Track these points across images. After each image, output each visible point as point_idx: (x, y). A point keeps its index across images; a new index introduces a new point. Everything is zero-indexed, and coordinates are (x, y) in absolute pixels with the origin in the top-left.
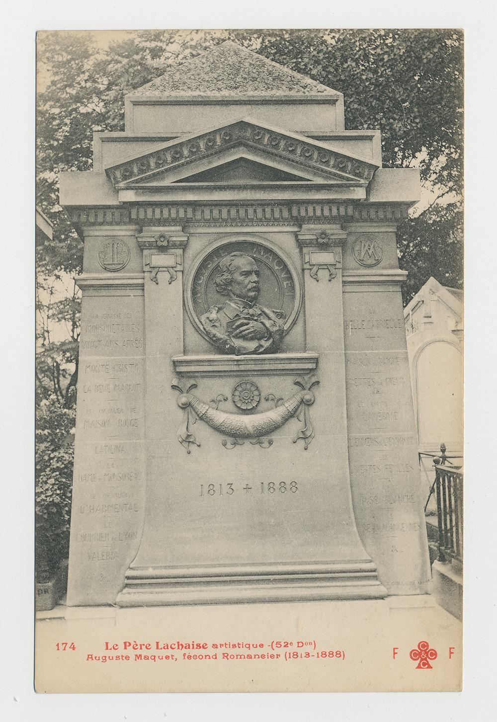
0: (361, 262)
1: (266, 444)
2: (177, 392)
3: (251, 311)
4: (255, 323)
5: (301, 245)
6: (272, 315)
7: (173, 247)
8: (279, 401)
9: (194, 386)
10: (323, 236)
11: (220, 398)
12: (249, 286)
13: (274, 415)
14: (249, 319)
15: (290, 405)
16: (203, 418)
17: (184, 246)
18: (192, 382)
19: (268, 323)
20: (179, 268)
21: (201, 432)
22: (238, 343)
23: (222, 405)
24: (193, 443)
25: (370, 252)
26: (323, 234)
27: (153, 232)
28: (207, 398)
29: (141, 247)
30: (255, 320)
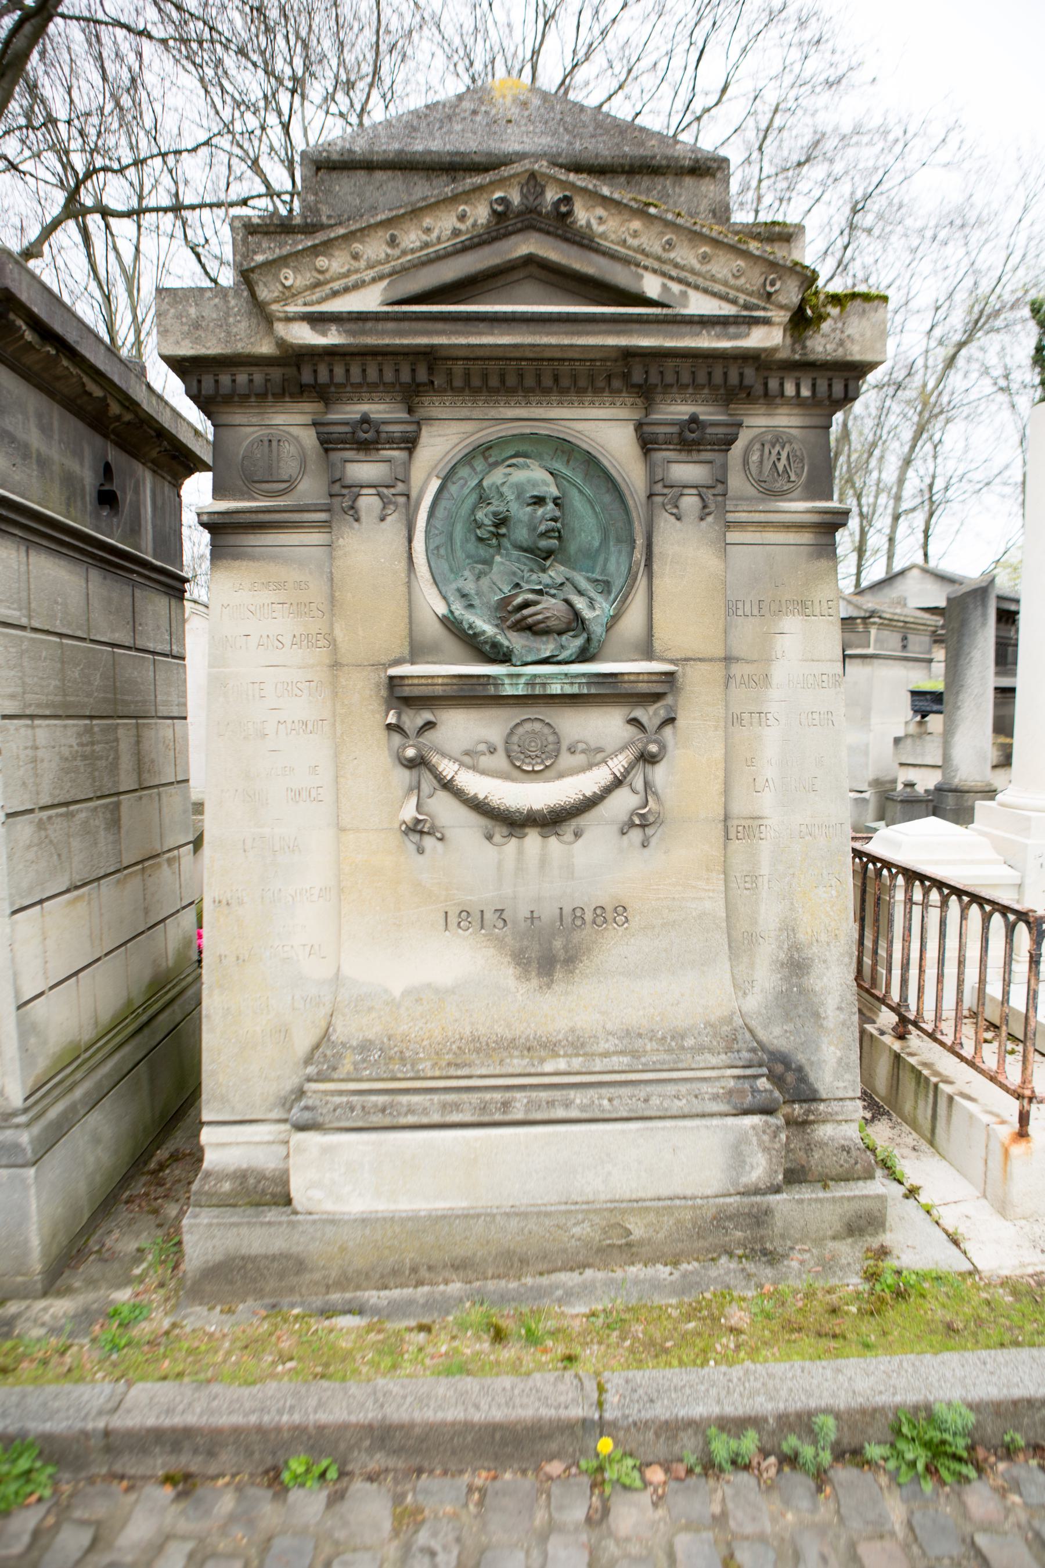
1: (569, 836)
2: (397, 738)
3: (545, 578)
4: (554, 601)
5: (647, 444)
6: (584, 584)
8: (595, 756)
9: (429, 725)
10: (694, 426)
11: (482, 747)
12: (542, 528)
13: (590, 782)
14: (540, 592)
15: (618, 764)
16: (447, 786)
17: (410, 443)
18: (427, 716)
19: (580, 603)
20: (400, 487)
21: (445, 810)
22: (515, 641)
24: (428, 833)
25: (781, 468)
26: (694, 419)
29: (328, 443)
30: (553, 596)
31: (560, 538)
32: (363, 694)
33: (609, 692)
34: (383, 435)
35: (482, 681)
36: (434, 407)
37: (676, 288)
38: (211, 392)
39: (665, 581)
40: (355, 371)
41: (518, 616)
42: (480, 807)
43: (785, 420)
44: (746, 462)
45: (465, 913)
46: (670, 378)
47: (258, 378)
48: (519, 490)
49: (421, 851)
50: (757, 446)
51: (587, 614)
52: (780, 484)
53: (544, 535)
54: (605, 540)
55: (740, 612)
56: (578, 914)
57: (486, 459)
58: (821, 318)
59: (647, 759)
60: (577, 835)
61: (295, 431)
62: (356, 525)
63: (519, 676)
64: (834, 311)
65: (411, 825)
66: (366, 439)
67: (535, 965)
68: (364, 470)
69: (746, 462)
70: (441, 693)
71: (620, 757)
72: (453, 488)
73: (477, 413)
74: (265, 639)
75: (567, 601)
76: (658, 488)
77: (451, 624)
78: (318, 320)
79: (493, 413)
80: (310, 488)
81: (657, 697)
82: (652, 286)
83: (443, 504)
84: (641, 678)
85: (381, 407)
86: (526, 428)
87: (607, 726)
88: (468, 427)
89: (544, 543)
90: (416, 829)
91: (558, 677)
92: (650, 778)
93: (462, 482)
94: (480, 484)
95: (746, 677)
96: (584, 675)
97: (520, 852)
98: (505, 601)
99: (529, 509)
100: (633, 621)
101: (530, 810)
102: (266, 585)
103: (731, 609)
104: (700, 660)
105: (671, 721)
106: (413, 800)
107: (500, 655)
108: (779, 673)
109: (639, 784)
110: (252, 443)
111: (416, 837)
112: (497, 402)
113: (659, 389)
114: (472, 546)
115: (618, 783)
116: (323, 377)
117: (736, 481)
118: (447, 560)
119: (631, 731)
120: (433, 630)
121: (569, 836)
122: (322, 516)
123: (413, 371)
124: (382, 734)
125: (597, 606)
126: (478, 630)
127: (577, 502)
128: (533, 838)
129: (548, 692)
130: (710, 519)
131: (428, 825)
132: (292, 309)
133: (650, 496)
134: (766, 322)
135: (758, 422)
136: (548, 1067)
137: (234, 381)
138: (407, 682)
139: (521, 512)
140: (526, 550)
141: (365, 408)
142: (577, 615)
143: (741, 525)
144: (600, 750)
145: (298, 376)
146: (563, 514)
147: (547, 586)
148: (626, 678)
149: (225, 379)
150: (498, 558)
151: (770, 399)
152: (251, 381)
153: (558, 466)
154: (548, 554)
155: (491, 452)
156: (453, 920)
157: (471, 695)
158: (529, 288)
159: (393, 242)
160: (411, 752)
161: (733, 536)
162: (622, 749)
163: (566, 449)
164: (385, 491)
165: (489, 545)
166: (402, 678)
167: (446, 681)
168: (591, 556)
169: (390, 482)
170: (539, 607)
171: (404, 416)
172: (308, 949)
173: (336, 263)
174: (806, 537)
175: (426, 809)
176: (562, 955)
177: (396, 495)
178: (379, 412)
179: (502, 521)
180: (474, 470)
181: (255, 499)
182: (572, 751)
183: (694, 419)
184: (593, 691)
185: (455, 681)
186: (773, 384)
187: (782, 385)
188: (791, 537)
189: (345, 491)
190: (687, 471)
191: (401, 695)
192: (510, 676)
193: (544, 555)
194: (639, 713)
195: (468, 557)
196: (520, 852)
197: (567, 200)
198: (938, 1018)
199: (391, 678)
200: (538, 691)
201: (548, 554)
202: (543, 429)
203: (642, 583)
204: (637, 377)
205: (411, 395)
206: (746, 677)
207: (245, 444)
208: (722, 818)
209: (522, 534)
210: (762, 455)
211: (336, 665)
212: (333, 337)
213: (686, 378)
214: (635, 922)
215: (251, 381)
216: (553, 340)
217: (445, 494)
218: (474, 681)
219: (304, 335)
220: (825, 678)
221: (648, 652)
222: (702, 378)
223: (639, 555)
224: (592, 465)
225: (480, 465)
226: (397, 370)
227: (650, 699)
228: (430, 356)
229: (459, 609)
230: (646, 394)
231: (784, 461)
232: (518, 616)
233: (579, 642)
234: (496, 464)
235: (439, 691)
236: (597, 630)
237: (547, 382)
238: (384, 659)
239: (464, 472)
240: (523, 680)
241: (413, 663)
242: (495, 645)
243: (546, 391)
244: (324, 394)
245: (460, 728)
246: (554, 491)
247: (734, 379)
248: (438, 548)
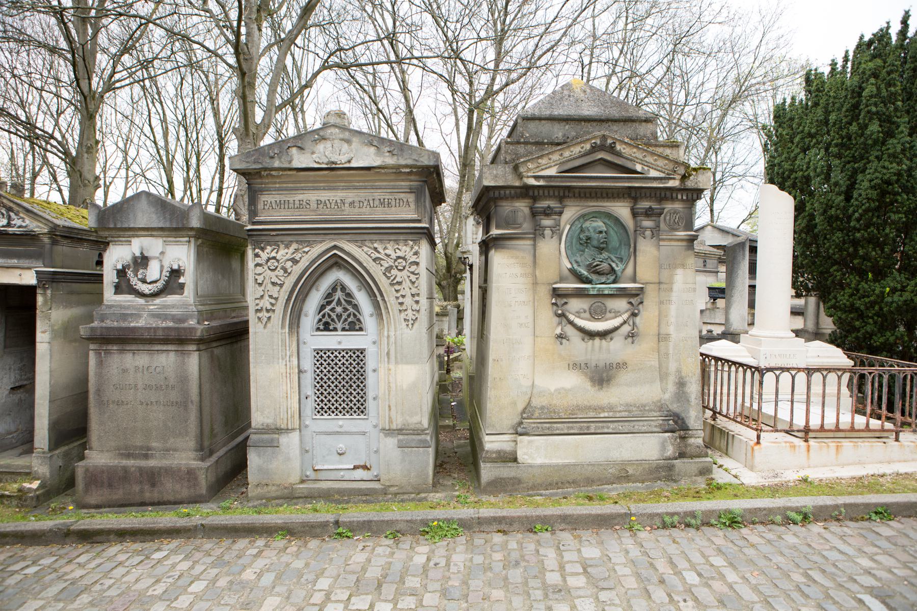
2: (555, 307)
5: (634, 214)
6: (614, 259)
8: (617, 314)
9: (566, 303)
13: (616, 322)
15: (625, 316)
16: (571, 323)
17: (560, 213)
18: (565, 300)
19: (614, 265)
21: (570, 330)
22: (594, 277)
23: (583, 315)
26: (650, 208)
27: (543, 204)
28: (573, 310)
29: (534, 213)
32: (544, 292)
33: (623, 293)
36: (568, 202)
37: (646, 168)
39: (640, 258)
40: (546, 192)
43: (678, 206)
44: (665, 219)
46: (643, 195)
47: (513, 192)
48: (595, 229)
49: (561, 344)
51: (616, 269)
52: (676, 226)
54: (620, 244)
56: (611, 365)
58: (690, 175)
59: (634, 315)
60: (611, 339)
64: (694, 173)
66: (548, 212)
68: (546, 222)
69: (665, 219)
72: (573, 228)
73: (581, 204)
77: (573, 271)
78: (537, 178)
79: (586, 204)
81: (637, 295)
82: (639, 168)
87: (621, 304)
88: (578, 208)
89: (602, 246)
90: (560, 337)
91: (607, 288)
97: (593, 344)
98: (591, 264)
100: (629, 270)
103: (661, 267)
105: (642, 303)
107: (589, 281)
108: (676, 287)
109: (631, 323)
114: (578, 246)
115: (625, 322)
116: (536, 193)
117: (662, 225)
119: (628, 306)
120: (566, 272)
121: (609, 340)
124: (550, 306)
127: (612, 232)
128: (597, 340)
132: (529, 174)
133: (635, 231)
134: (674, 179)
135: (669, 206)
136: (602, 415)
142: (613, 269)
143: (663, 240)
145: (526, 192)
149: (502, 192)
151: (673, 199)
153: (606, 221)
154: (603, 249)
156: (571, 366)
157: (580, 294)
158: (600, 167)
159: (561, 155)
160: (560, 312)
161: (661, 243)
162: (626, 311)
163: (609, 216)
168: (616, 249)
173: (543, 161)
174: (684, 244)
177: (556, 230)
179: (589, 238)
182: (610, 312)
183: (650, 208)
186: (674, 195)
188: (680, 243)
190: (647, 223)
191: (556, 293)
194: (631, 300)
196: (593, 344)
197: (614, 143)
198: (728, 409)
199: (554, 289)
201: (603, 249)
202: (602, 210)
203: (632, 258)
204: (633, 195)
205: (561, 199)
209: (595, 243)
212: (541, 183)
213: (648, 195)
214: (630, 368)
216: (608, 184)
219: (532, 182)
221: (634, 281)
222: (653, 195)
223: (632, 250)
224: (617, 221)
225: (581, 220)
227: (635, 296)
228: (569, 188)
229: (575, 266)
230: (635, 200)
233: (613, 277)
236: (619, 273)
237: (604, 195)
239: (577, 223)
242: (587, 278)
243: (603, 198)
245: (575, 304)
247: (663, 195)
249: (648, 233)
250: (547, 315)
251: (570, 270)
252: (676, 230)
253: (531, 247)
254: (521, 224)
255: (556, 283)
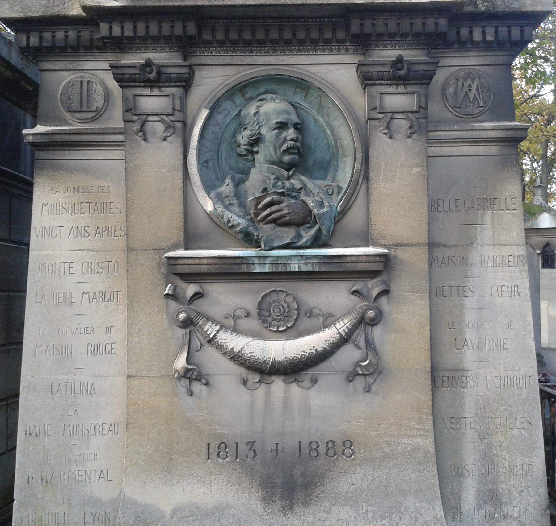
0: (457, 109)
1: (306, 383)
2: (173, 305)
3: (287, 184)
4: (293, 201)
7: (167, 84)
8: (328, 320)
12: (284, 147)
15: (342, 326)
17: (186, 83)
23: (244, 323)
24: (196, 379)
25: (471, 96)
26: (400, 59)
30: (294, 197)
31: (300, 154)
32: (149, 270)
34: (163, 77)
35: (237, 261)
38: (37, 44)
41: (266, 213)
42: (236, 358)
45: (223, 446)
47: (72, 35)
50: (453, 81)
52: (472, 109)
53: (287, 151)
55: (441, 209)
56: (313, 446)
57: (243, 95)
60: (314, 381)
61: (101, 74)
62: (144, 143)
63: (265, 257)
65: (182, 373)
67: (279, 489)
70: (206, 271)
71: (346, 321)
72: (219, 117)
73: (237, 60)
74: (75, 229)
75: (303, 201)
76: (374, 115)
80: (115, 119)
81: (374, 274)
83: (212, 128)
84: (360, 259)
85: (163, 55)
86: (272, 71)
87: (335, 297)
88: (229, 71)
91: (296, 259)
92: (370, 337)
93: (226, 112)
94: (239, 114)
95: (446, 259)
96: (315, 256)
99: (276, 131)
101: (274, 362)
102: (77, 190)
104: (409, 245)
105: (385, 292)
106: (184, 355)
109: (362, 342)
110: (68, 83)
111: (185, 382)
112: (251, 51)
113: (374, 38)
115: (343, 341)
117: (436, 108)
118: (214, 171)
119: (354, 298)
121: (306, 383)
122: (120, 138)
123: (185, 26)
124: (161, 301)
125: (326, 204)
126: (235, 223)
128: (278, 385)
129: (288, 270)
130: (415, 136)
131: (195, 373)
137: (54, 37)
138: (180, 262)
139: (269, 134)
140: (273, 163)
141: (151, 55)
143: (439, 141)
144: (331, 315)
146: (303, 136)
147: (288, 190)
148: (349, 259)
150: (253, 171)
151: (464, 45)
152: (66, 37)
155: (247, 89)
156: (214, 449)
157: (230, 272)
162: (346, 315)
164: (165, 118)
165: (246, 160)
166: (176, 258)
167: (210, 261)
169: (170, 111)
170: (283, 205)
171: (180, 62)
172: (98, 473)
175: (195, 360)
176: (300, 481)
178: (161, 59)
180: (235, 103)
181: (70, 125)
184: (323, 269)
185: (216, 261)
186: (464, 32)
187: (471, 32)
188: (481, 149)
189: (135, 118)
192: (259, 257)
193: (287, 167)
194: (358, 286)
195: (231, 168)
196: (268, 395)
200: (280, 269)
202: (285, 71)
203: (364, 187)
206: (446, 259)
207: (63, 84)
208: (429, 369)
210: (456, 88)
211: (129, 249)
215: (66, 37)
217: (212, 122)
218: (231, 261)
220: (511, 258)
225: (239, 99)
226: (172, 27)
231: (474, 91)
232: (266, 213)
233: (313, 231)
234: (251, 99)
235: (204, 269)
238: (164, 244)
240: (268, 261)
241: (186, 249)
244: (119, 45)
246: (294, 118)
248: (207, 162)
249: (402, 124)
250: (158, 321)
251: (209, 216)
252: (473, 117)
253: (121, 165)
254: (98, 114)
255: (175, 247)
